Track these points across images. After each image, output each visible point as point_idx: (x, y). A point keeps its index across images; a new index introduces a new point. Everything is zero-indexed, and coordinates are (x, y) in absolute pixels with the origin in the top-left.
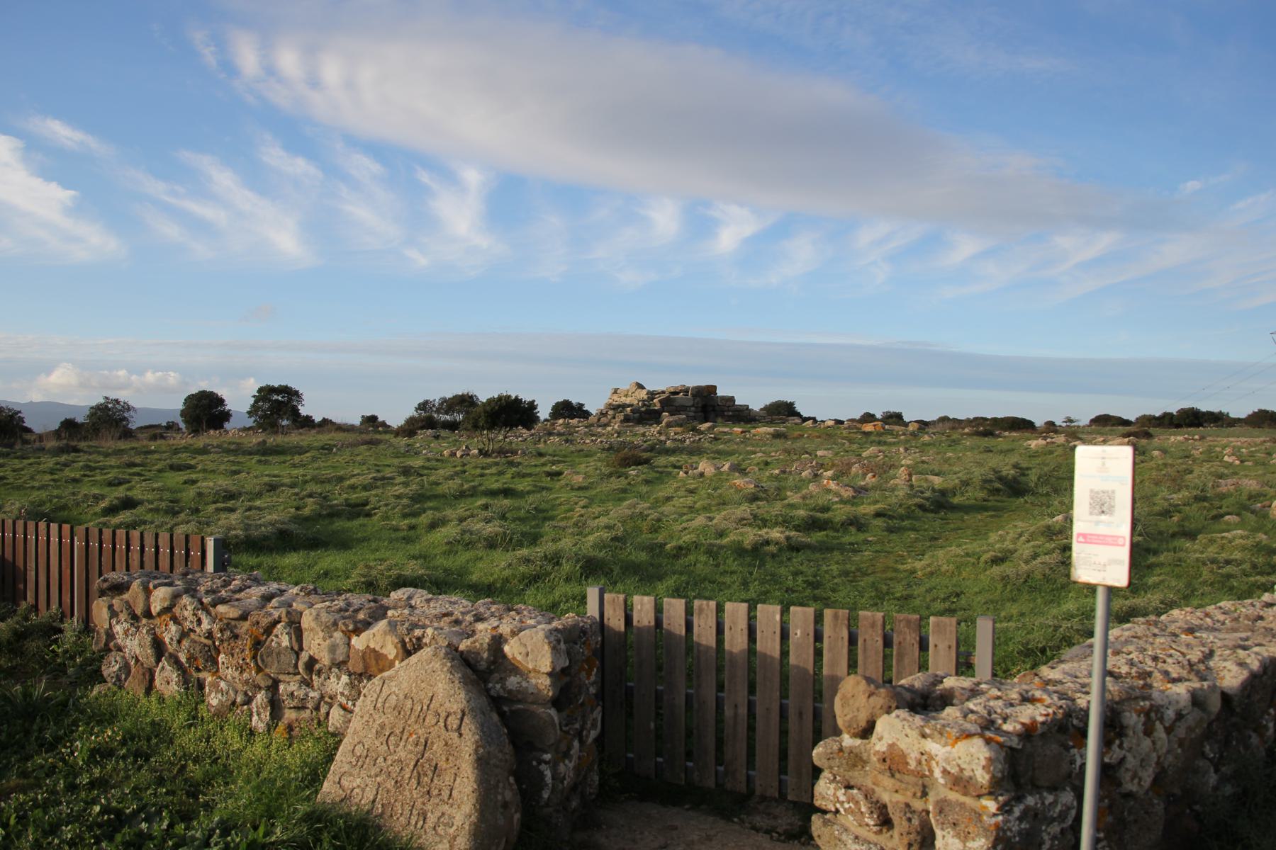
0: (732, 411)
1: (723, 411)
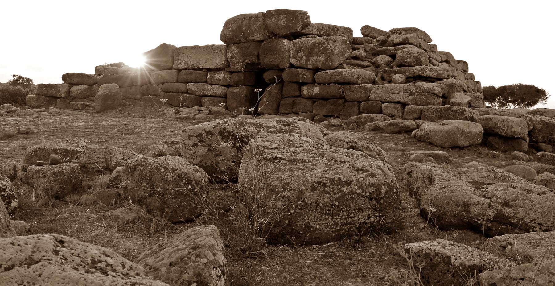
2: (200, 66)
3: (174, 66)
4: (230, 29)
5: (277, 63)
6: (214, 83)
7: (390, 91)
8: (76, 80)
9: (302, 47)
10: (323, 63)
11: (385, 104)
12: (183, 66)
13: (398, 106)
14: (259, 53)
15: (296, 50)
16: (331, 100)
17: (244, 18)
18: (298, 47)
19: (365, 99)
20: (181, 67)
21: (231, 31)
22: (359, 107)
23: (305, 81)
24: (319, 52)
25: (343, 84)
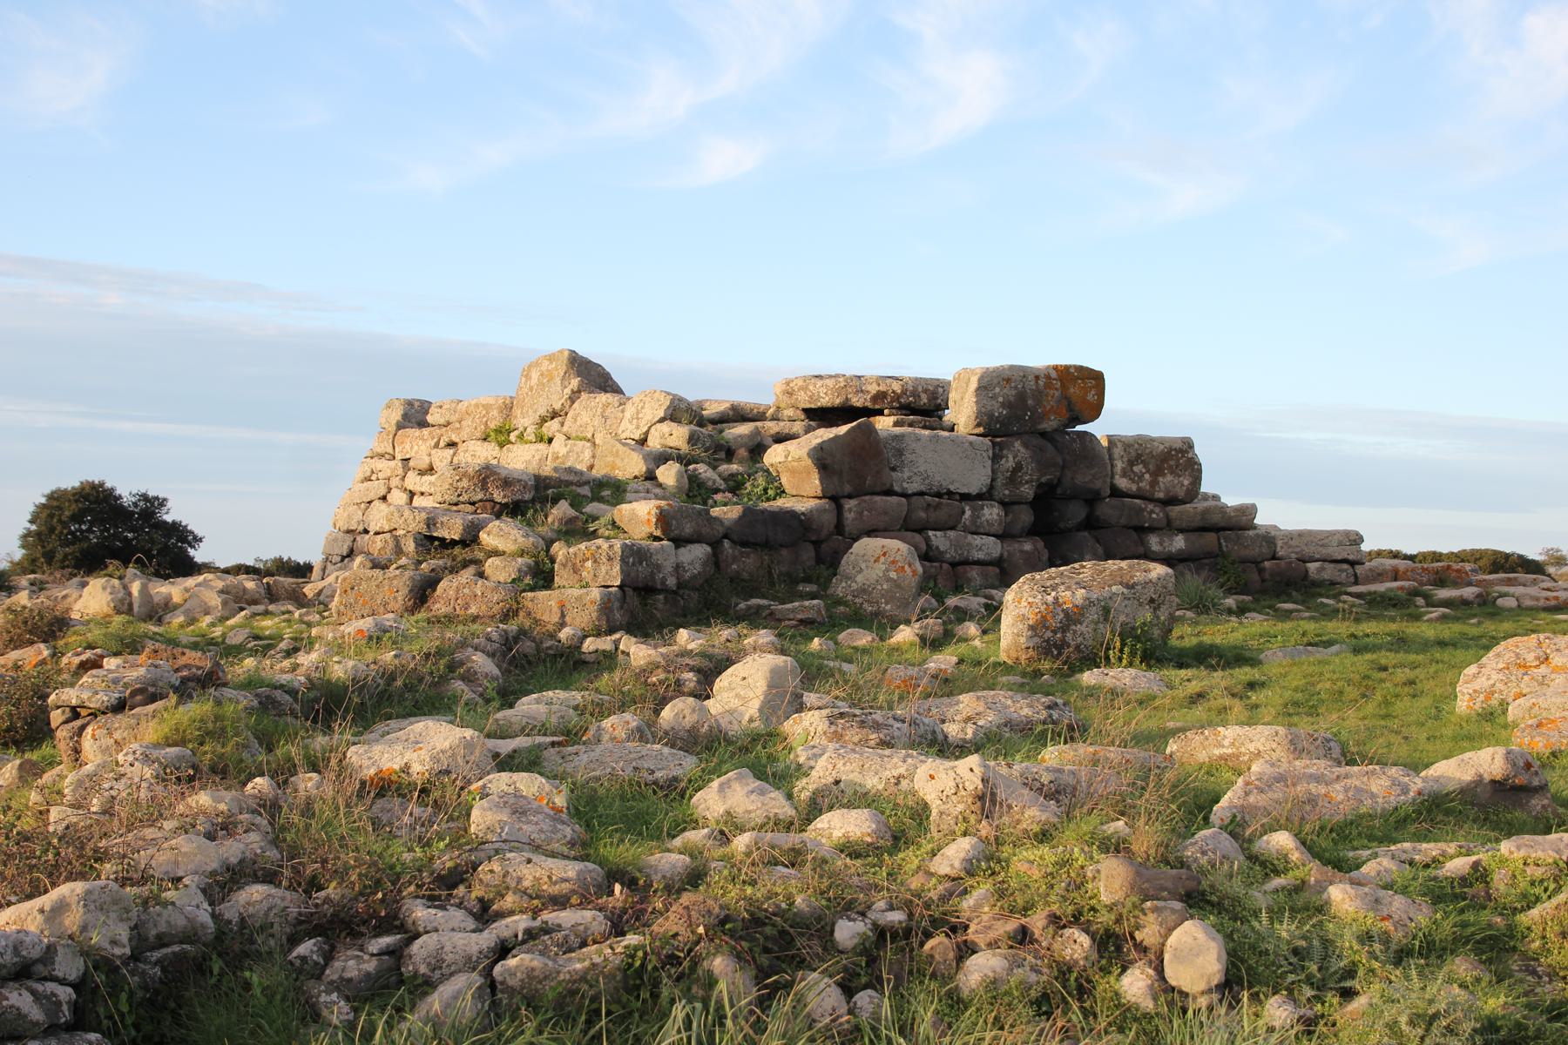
0: (1181, 531)
1: (1142, 530)
2: (952, 488)
3: (896, 488)
4: (1001, 399)
5: (1098, 484)
6: (982, 530)
7: (1320, 543)
8: (688, 529)
9: (1141, 455)
10: (1188, 489)
11: (1317, 564)
12: (915, 485)
13: (1345, 566)
14: (1064, 460)
15: (1129, 460)
16: (1206, 561)
17: (1024, 376)
18: (1133, 454)
19: (1269, 556)
20: (912, 487)
21: (1003, 405)
22: (1261, 571)
23: (1156, 525)
24: (1177, 466)
25: (1217, 529)
